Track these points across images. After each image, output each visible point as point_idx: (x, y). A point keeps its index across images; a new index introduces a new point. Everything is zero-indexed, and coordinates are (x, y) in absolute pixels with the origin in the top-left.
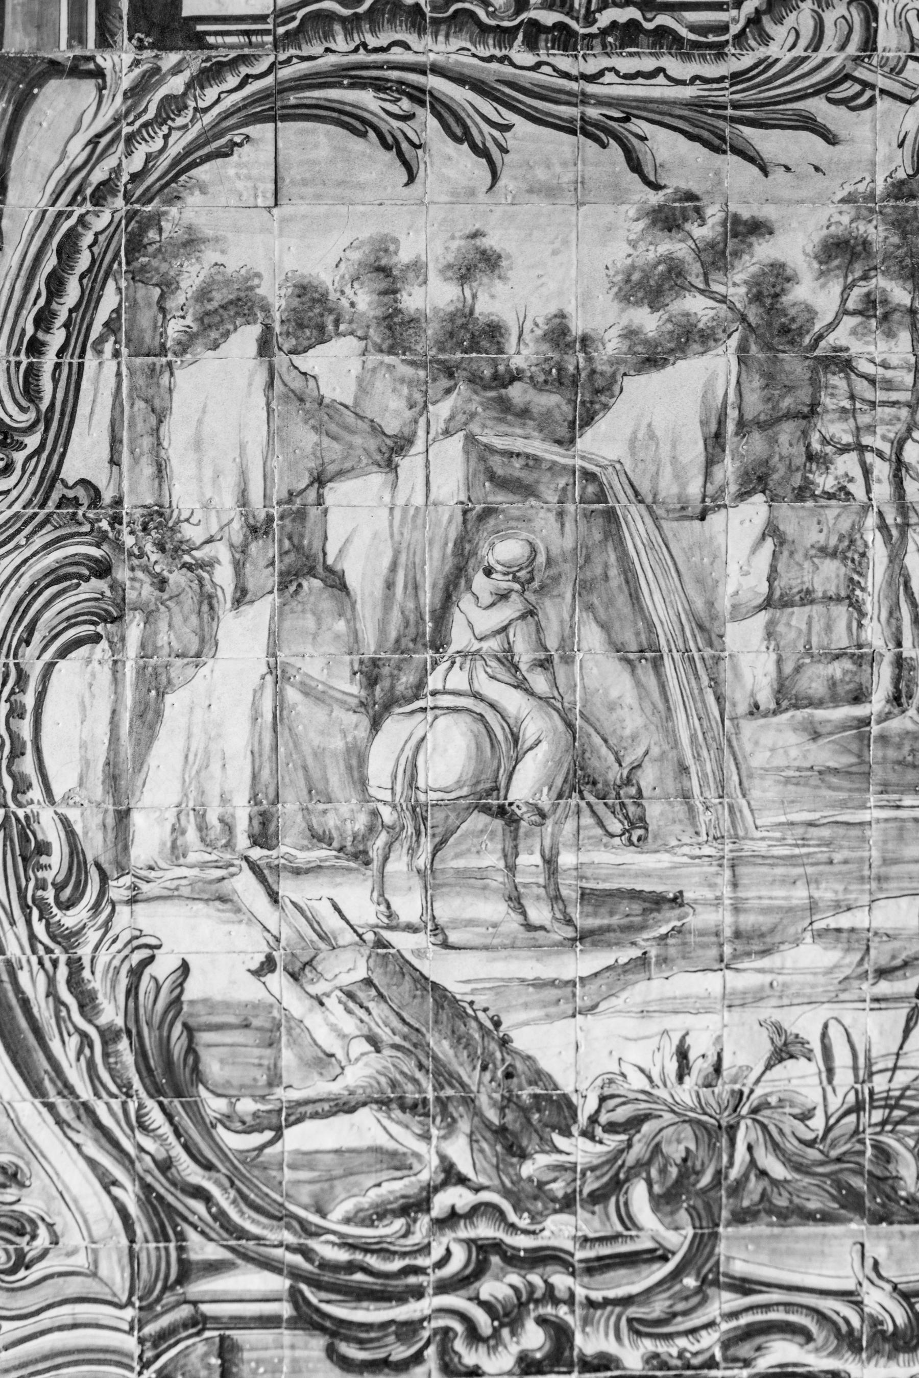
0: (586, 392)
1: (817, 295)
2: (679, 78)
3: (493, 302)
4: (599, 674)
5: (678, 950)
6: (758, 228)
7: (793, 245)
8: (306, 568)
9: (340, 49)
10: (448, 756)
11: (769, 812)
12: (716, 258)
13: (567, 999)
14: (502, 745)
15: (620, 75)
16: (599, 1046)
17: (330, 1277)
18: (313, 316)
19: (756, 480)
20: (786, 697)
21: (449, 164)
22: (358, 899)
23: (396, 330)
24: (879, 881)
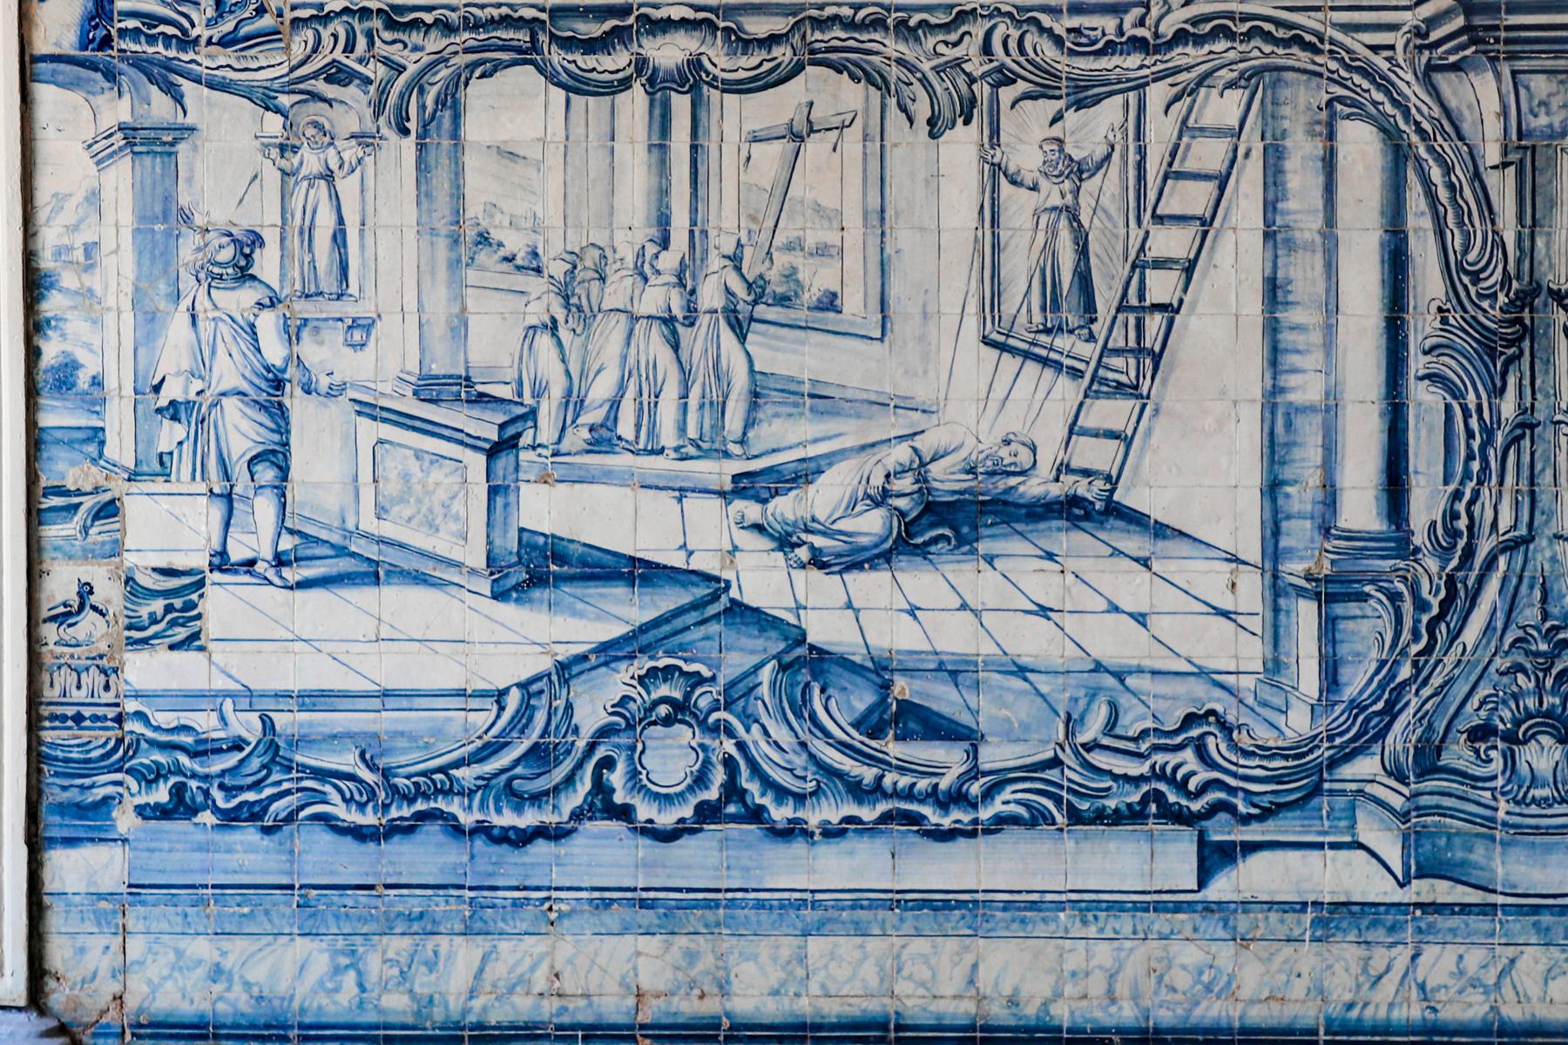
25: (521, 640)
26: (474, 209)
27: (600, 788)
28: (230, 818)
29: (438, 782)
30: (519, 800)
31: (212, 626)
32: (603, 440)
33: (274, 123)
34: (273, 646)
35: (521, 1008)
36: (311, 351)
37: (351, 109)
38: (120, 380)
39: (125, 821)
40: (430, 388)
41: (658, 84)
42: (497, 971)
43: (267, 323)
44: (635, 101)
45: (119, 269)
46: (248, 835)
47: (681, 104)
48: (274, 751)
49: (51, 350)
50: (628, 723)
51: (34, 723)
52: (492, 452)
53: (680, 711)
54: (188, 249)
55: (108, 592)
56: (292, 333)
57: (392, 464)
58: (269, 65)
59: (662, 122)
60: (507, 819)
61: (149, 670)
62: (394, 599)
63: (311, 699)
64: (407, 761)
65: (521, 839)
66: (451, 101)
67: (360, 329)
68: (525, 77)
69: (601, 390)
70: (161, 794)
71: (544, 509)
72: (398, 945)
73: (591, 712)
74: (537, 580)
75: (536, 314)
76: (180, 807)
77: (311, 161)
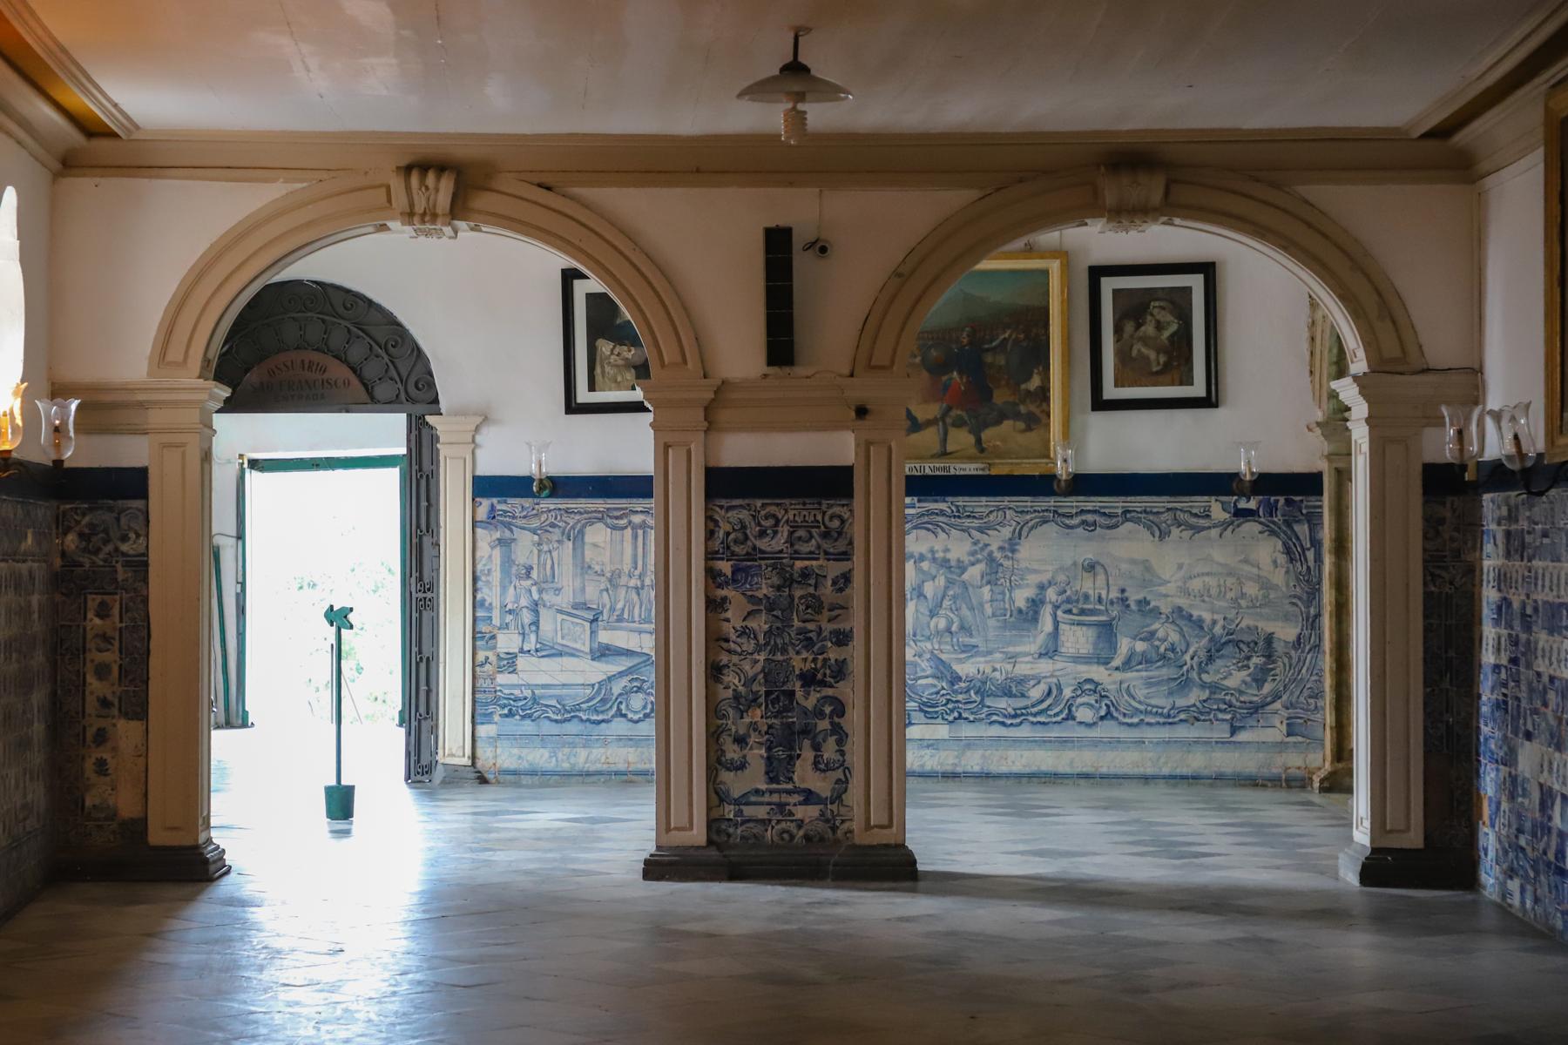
0: (963, 570)
1: (998, 555)
2: (976, 523)
3: (949, 556)
4: (965, 612)
5: (977, 654)
6: (987, 545)
7: (994, 547)
8: (921, 595)
9: (926, 519)
10: (942, 624)
11: (991, 634)
12: (982, 549)
13: (960, 661)
14: (951, 622)
15: (967, 522)
16: (966, 669)
17: (924, 704)
18: (922, 558)
19: (989, 582)
20: (994, 615)
21: (942, 535)
22: (929, 646)
23: (934, 560)
24: (1009, 644)
25: (597, 671)
26: (587, 559)
27: (619, 709)
28: (523, 717)
29: (577, 708)
30: (598, 712)
31: (519, 667)
32: (620, 619)
33: (536, 538)
34: (535, 673)
35: (598, 767)
36: (545, 597)
37: (556, 534)
38: (496, 604)
39: (496, 718)
40: (576, 606)
41: (635, 528)
42: (592, 757)
43: (534, 589)
44: (629, 532)
45: (496, 576)
46: (528, 722)
47: (640, 532)
48: (535, 700)
49: (479, 596)
50: (626, 693)
51: (474, 693)
52: (592, 622)
53: (639, 689)
54: (514, 570)
55: (493, 658)
56: (540, 591)
57: (566, 625)
58: (535, 523)
59: (635, 537)
60: (595, 717)
61: (502, 679)
62: (565, 659)
63: (544, 686)
64: (569, 703)
65: (600, 722)
66: (582, 532)
67: (558, 591)
68: (600, 525)
69: (620, 606)
70: (506, 711)
71: (604, 637)
72: (566, 750)
73: (617, 690)
74: (603, 655)
75: (603, 586)
76: (511, 714)
77: (545, 548)
